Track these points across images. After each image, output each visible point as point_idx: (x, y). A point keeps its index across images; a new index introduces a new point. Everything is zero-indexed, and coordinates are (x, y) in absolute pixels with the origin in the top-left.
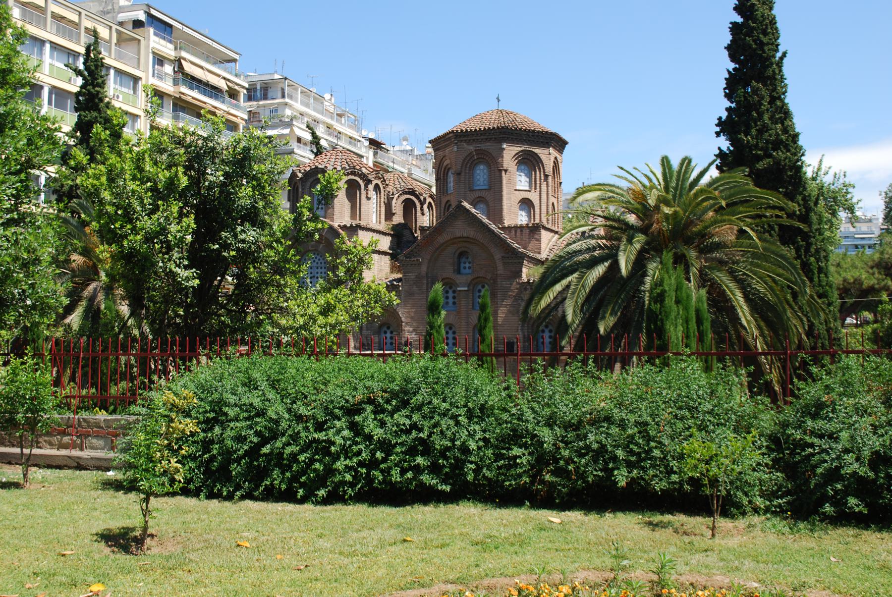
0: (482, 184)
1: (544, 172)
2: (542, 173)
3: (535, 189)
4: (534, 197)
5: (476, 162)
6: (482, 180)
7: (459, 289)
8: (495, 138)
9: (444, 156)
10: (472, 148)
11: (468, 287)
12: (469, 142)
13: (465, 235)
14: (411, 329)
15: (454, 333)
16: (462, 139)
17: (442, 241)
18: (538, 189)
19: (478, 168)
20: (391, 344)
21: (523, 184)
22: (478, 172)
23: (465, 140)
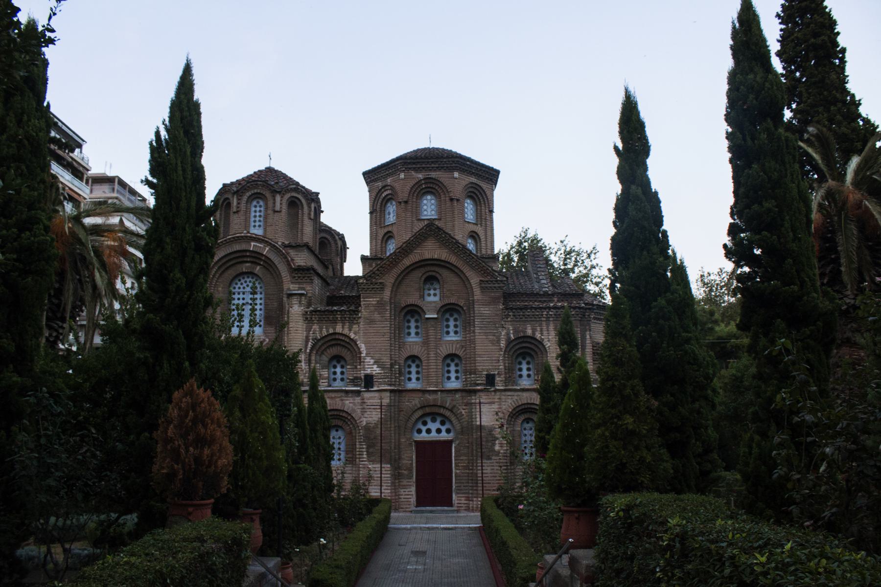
0: (429, 214)
4: (479, 230)
5: (424, 191)
6: (429, 210)
7: (427, 316)
8: (447, 167)
9: (384, 187)
10: (421, 176)
11: (437, 314)
12: (417, 170)
14: (372, 361)
15: (418, 366)
16: (409, 166)
19: (425, 198)
20: (342, 380)
21: (469, 218)
22: (425, 202)
23: (414, 168)
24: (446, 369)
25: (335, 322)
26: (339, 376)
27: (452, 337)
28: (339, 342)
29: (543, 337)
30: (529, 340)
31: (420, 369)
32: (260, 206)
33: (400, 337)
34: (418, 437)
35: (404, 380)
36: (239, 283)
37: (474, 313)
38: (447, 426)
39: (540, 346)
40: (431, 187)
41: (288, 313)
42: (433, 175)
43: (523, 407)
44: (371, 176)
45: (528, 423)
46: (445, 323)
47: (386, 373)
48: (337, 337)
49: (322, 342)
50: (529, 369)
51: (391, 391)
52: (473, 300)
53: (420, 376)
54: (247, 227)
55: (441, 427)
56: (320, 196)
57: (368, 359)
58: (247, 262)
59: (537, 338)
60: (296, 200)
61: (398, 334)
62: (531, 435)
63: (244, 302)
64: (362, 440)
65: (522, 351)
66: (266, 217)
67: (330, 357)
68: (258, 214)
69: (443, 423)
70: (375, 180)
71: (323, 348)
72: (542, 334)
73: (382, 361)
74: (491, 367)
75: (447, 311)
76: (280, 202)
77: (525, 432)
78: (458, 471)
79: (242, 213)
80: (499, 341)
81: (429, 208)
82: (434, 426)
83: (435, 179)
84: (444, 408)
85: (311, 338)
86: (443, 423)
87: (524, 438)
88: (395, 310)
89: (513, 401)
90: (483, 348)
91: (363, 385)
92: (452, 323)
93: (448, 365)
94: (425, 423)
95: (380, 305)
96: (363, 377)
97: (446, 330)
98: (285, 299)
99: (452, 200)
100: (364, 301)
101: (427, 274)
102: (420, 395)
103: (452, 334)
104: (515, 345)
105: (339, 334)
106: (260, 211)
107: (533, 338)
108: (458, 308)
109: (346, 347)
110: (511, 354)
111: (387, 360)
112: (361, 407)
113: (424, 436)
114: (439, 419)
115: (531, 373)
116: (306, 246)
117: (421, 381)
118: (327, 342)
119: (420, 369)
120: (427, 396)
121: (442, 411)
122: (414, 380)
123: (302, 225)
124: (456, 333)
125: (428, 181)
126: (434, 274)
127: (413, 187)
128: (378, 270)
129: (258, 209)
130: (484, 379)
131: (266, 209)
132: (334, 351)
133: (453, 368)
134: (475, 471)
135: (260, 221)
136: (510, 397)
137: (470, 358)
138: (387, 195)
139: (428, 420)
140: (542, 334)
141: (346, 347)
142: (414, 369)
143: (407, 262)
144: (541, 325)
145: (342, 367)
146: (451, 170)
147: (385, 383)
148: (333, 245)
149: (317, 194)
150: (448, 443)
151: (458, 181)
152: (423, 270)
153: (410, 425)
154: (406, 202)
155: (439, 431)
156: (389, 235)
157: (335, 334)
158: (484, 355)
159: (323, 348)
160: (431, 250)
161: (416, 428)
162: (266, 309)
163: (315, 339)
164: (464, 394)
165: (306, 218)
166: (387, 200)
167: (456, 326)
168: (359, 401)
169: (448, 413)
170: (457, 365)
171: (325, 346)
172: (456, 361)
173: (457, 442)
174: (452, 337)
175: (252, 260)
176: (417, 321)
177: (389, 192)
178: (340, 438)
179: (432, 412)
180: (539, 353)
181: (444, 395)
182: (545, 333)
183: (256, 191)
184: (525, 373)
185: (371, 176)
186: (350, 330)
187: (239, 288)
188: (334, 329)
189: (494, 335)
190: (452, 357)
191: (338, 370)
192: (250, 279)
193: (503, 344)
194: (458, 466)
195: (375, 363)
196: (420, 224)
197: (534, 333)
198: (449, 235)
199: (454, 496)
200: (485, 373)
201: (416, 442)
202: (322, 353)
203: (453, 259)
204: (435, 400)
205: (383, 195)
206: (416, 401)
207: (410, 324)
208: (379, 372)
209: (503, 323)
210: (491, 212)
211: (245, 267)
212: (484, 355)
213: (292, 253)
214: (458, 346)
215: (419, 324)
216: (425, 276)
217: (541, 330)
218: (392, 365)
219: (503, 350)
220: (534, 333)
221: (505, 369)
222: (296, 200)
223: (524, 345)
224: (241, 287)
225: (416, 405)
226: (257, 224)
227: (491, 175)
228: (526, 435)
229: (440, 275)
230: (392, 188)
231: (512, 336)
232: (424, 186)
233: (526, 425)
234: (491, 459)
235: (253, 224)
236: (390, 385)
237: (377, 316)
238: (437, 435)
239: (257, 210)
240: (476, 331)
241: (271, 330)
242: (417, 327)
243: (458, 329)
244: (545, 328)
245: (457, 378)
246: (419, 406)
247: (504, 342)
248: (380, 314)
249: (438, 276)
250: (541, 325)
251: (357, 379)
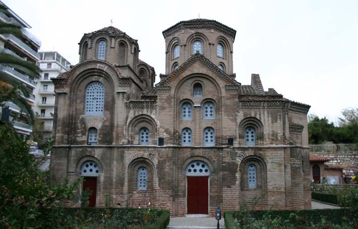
4: (225, 62)
7: (195, 105)
10: (193, 31)
11: (201, 104)
13: (200, 72)
14: (163, 130)
15: (189, 134)
17: (185, 76)
20: (147, 141)
22: (195, 46)
24: (206, 135)
25: (142, 108)
26: (145, 139)
27: (209, 117)
28: (145, 120)
30: (253, 119)
31: (190, 136)
32: (104, 45)
33: (179, 118)
34: (189, 174)
35: (181, 142)
36: (91, 87)
38: (206, 168)
39: (259, 123)
40: (198, 38)
42: (200, 31)
43: (249, 157)
44: (166, 33)
45: (252, 167)
46: (205, 110)
48: (144, 117)
49: (135, 119)
50: (252, 136)
51: (174, 147)
53: (190, 139)
54: (96, 56)
55: (202, 168)
56: (138, 42)
58: (95, 75)
60: (124, 42)
61: (178, 116)
62: (254, 174)
63: (93, 97)
65: (248, 126)
66: (106, 51)
67: (140, 128)
68: (102, 49)
69: (203, 166)
70: (169, 35)
71: (136, 123)
75: (206, 103)
76: (114, 43)
77: (250, 172)
78: (212, 194)
79: (93, 49)
80: (235, 119)
81: (197, 47)
82: (198, 168)
83: (200, 33)
84: (204, 157)
86: (203, 166)
87: (249, 176)
88: (177, 102)
91: (158, 144)
92: (209, 110)
93: (207, 133)
94: (193, 166)
95: (169, 99)
97: (205, 113)
98: (116, 96)
99: (210, 44)
101: (197, 82)
102: (189, 150)
103: (209, 116)
104: (245, 122)
105: (145, 115)
106: (104, 48)
107: (255, 118)
108: (212, 101)
109: (149, 123)
110: (242, 127)
113: (192, 174)
114: (201, 164)
115: (253, 138)
116: (128, 66)
117: (191, 142)
118: (138, 119)
119: (190, 136)
120: (194, 151)
121: (202, 159)
122: (187, 141)
123: (127, 56)
124: (211, 115)
125: (197, 34)
126: (199, 82)
127: (189, 37)
128: (167, 79)
129: (102, 47)
130: (227, 141)
131: (107, 46)
132: (143, 125)
133: (209, 135)
134: (221, 194)
135: (103, 53)
138: (175, 43)
139: (195, 164)
141: (149, 123)
142: (187, 135)
143: (184, 74)
144: (260, 111)
145: (147, 134)
146: (209, 28)
147: (170, 143)
148: (148, 72)
149: (137, 41)
150: (207, 178)
151: (213, 35)
152: (193, 80)
153: (184, 167)
154: (185, 46)
155: (201, 171)
156: (176, 64)
157: (143, 115)
159: (136, 123)
160: (198, 68)
161: (188, 169)
162: (105, 101)
164: (215, 150)
165: (129, 53)
166: (175, 46)
167: (211, 111)
169: (206, 161)
170: (211, 133)
171: (137, 122)
172: (212, 131)
174: (209, 117)
175: (98, 74)
176: (189, 108)
177: (176, 41)
178: (145, 174)
179: (196, 160)
180: (259, 127)
181: (204, 150)
182: (262, 115)
183: (101, 37)
184: (250, 138)
185: (166, 33)
186: (151, 113)
187: (91, 90)
188: (142, 112)
190: (209, 128)
191: (145, 135)
192: (97, 85)
195: (165, 131)
197: (256, 115)
198: (208, 60)
199: (209, 208)
201: (188, 177)
202: (135, 126)
203: (210, 74)
204: (199, 153)
205: (173, 43)
206: (188, 153)
207: (185, 110)
209: (238, 109)
210: (232, 52)
211: (94, 78)
213: (120, 70)
214: (212, 122)
215: (191, 110)
216: (194, 83)
217: (260, 114)
218: (174, 133)
222: (124, 42)
223: (250, 122)
224: (92, 89)
225: (188, 156)
226: (102, 55)
227: (232, 33)
228: (250, 174)
229: (203, 83)
230: (178, 39)
232: (195, 37)
233: (250, 168)
234: (231, 187)
235: (99, 55)
236: (174, 144)
237: (166, 105)
238: (199, 173)
239: (102, 46)
241: (108, 113)
242: (189, 112)
243: (212, 113)
245: (212, 141)
246: (190, 156)
249: (201, 83)
250: (260, 111)
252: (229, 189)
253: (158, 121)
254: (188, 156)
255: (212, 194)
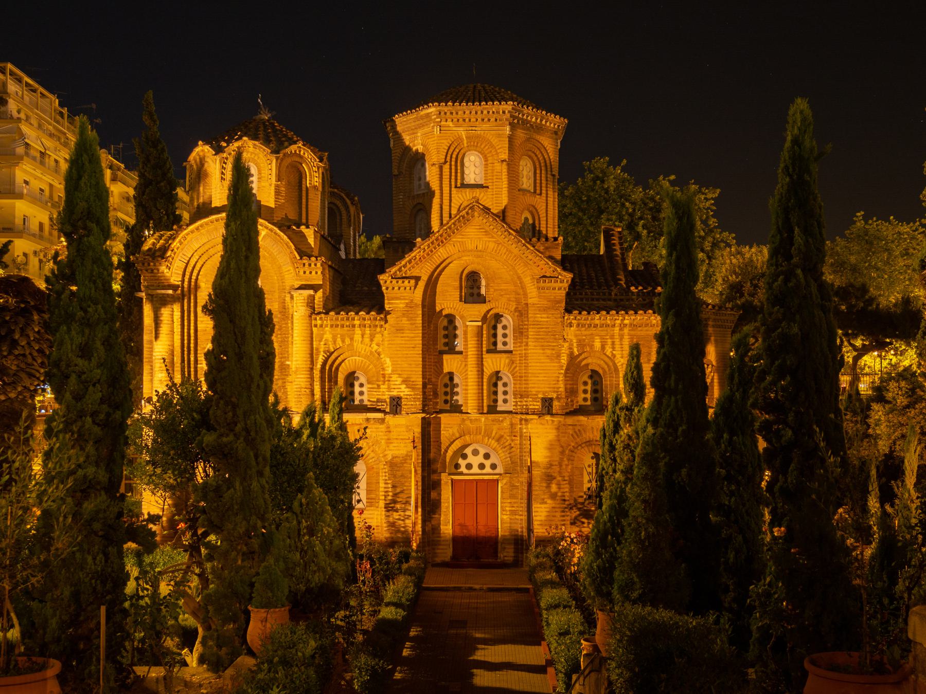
1: (551, 171)
2: (549, 173)
3: (540, 194)
14: (400, 380)
18: (544, 195)
29: (614, 352)
37: (528, 321)
41: (292, 318)
47: (417, 395)
52: (527, 304)
57: (394, 377)
59: (607, 354)
64: (387, 478)
72: (613, 348)
73: (412, 380)
74: (548, 389)
78: (505, 517)
85: (322, 350)
89: (575, 432)
90: (538, 364)
96: (388, 400)
100: (389, 303)
111: (419, 381)
112: (386, 437)
136: (571, 427)
137: (520, 377)
140: (613, 348)
158: (539, 373)
163: (328, 351)
168: (383, 430)
173: (504, 481)
182: (617, 346)
189: (553, 349)
193: (564, 360)
194: (506, 511)
195: (404, 382)
196: (460, 196)
197: (603, 347)
200: (541, 396)
208: (409, 393)
212: (539, 373)
217: (613, 343)
219: (564, 368)
220: (603, 347)
221: (566, 392)
231: (575, 350)
240: (529, 343)
244: (617, 342)
247: (565, 358)
248: (408, 320)
251: (382, 402)
252: (543, 506)
253: (388, 360)
254: (453, 434)
255: (505, 517)
